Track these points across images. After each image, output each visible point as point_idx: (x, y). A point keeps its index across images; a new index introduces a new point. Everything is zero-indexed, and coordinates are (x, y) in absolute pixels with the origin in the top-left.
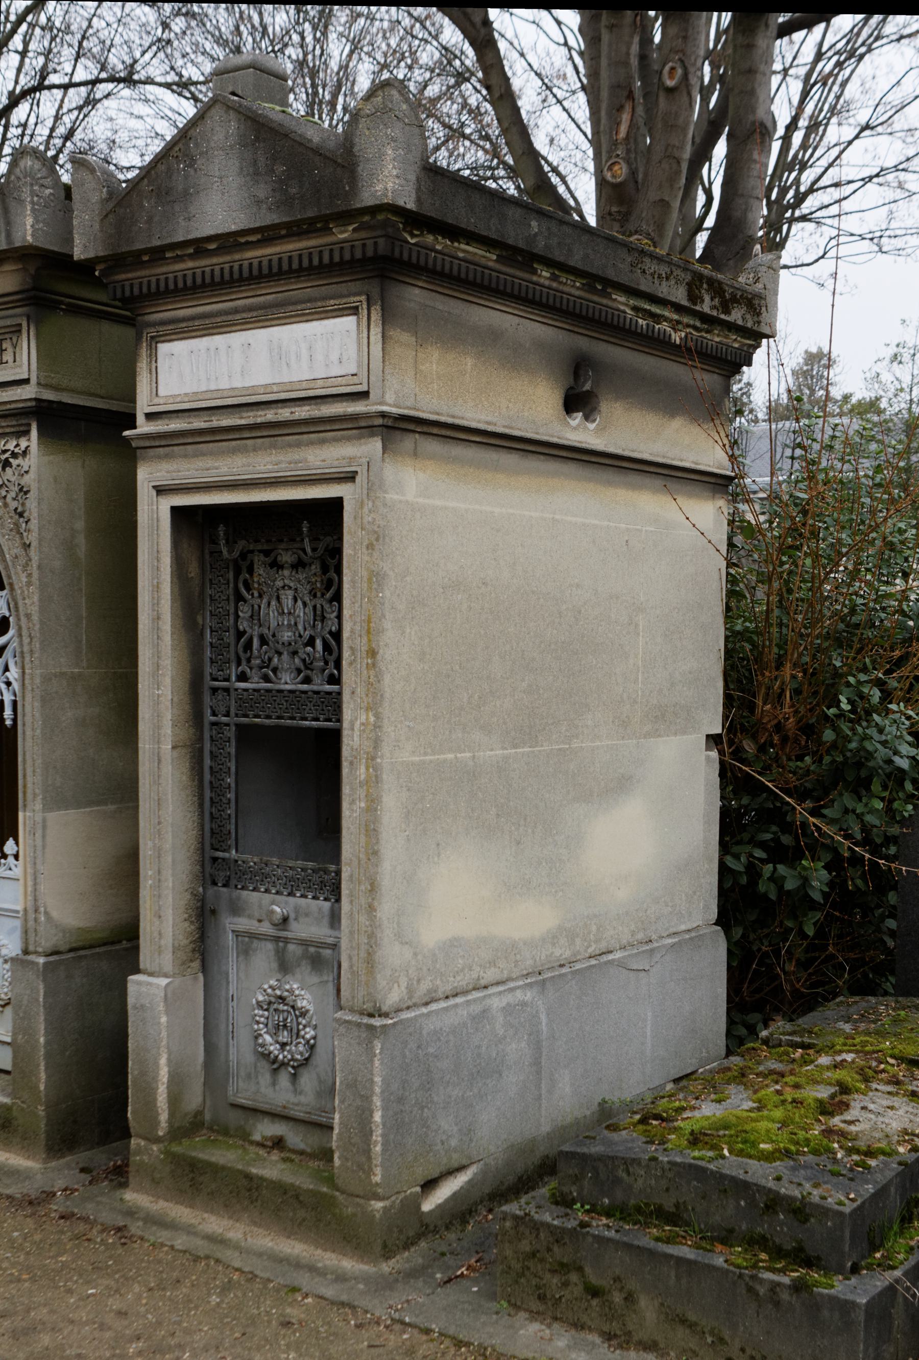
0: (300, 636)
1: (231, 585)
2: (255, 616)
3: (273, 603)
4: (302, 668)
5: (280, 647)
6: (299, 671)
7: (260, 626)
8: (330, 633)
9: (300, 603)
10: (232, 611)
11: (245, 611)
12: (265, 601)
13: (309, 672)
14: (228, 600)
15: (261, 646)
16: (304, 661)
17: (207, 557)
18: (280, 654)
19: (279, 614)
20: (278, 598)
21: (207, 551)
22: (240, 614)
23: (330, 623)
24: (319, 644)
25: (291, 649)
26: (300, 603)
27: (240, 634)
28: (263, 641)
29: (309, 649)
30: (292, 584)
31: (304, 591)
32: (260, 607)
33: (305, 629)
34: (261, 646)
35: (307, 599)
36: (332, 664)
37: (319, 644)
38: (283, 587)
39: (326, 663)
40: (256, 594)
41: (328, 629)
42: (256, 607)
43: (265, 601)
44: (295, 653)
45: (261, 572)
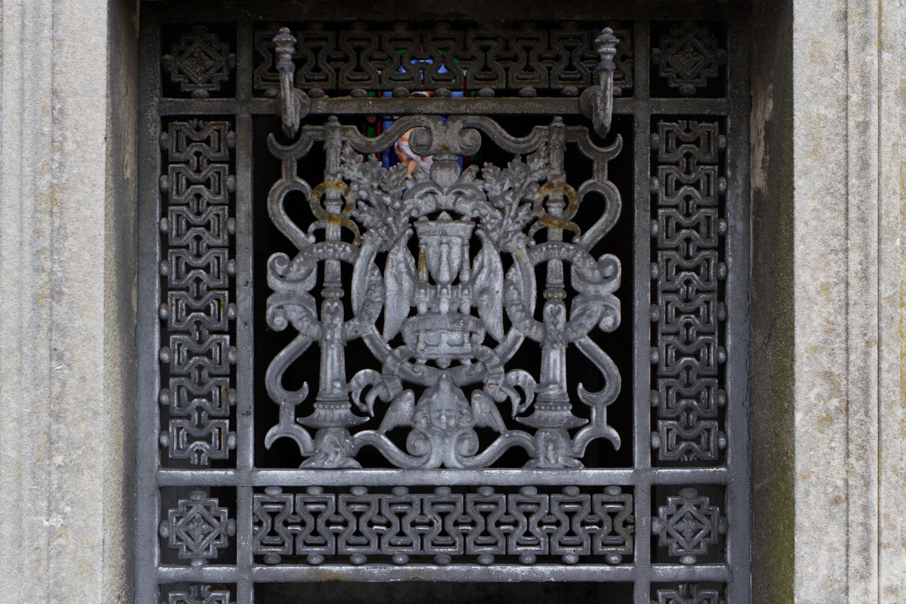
0: (490, 342)
1: (245, 207)
2: (332, 289)
3: (399, 256)
4: (499, 424)
5: (421, 372)
6: (486, 436)
7: (349, 315)
8: (596, 334)
9: (490, 256)
10: (245, 276)
11: (289, 280)
12: (368, 250)
13: (523, 437)
14: (232, 248)
15: (350, 372)
16: (504, 407)
17: (154, 129)
18: (419, 390)
19: (417, 284)
20: (414, 245)
21: (153, 115)
22: (273, 281)
23: (596, 308)
24: (555, 363)
25: (464, 376)
26: (490, 256)
27: (268, 342)
28: (357, 355)
29: (522, 376)
30: (465, 207)
31: (507, 228)
32: (347, 269)
33: (507, 325)
34: (350, 372)
35: (517, 245)
36: (599, 414)
37: (555, 363)
38: (433, 216)
39: (581, 410)
40: (333, 231)
41: (589, 325)
42: (334, 267)
43: (368, 250)
44: (469, 390)
45: (353, 173)
